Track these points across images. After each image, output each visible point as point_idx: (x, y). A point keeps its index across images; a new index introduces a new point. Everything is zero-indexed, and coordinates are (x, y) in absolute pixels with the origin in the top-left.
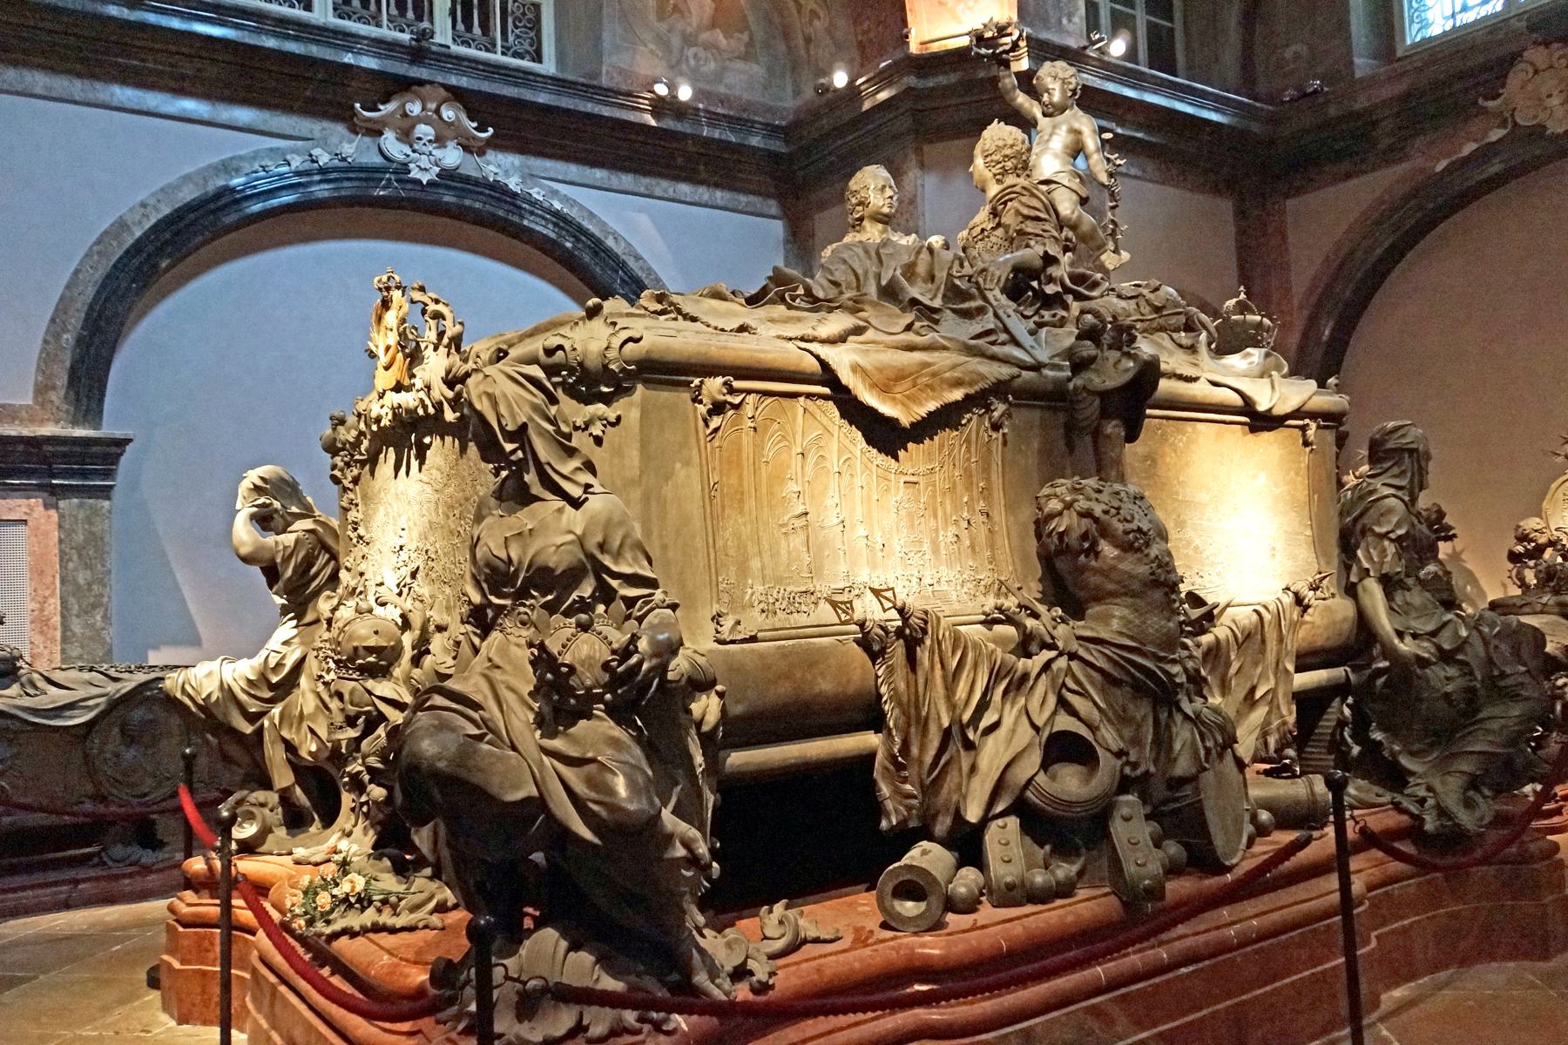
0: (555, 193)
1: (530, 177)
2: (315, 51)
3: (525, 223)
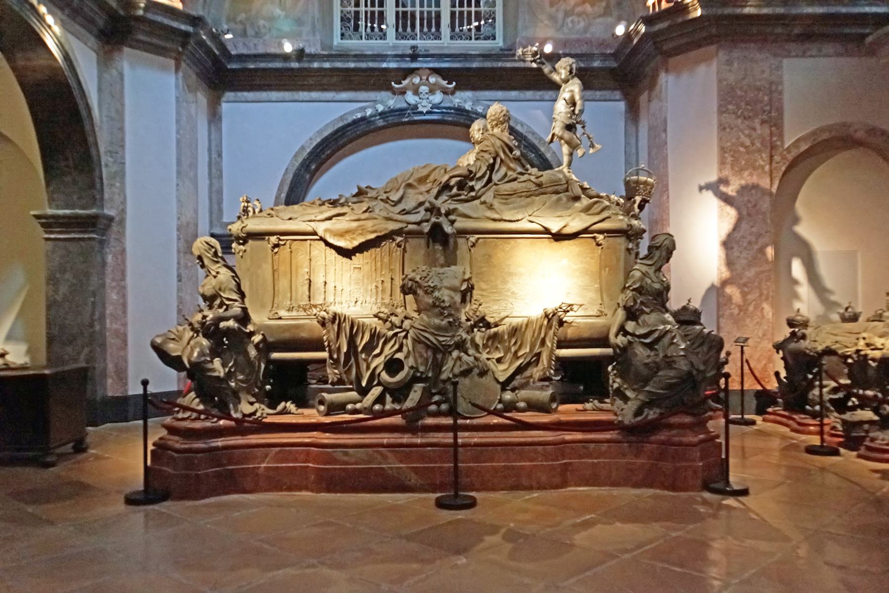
2: (371, 65)
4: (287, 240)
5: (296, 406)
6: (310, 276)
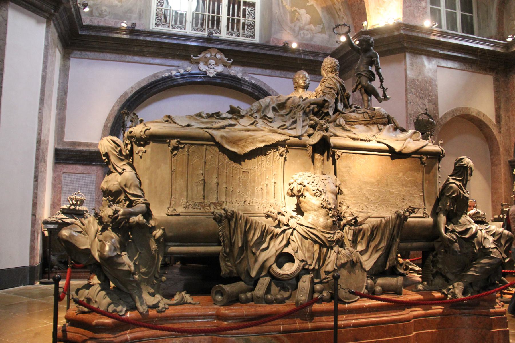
0: (253, 78)
1: (245, 73)
3: (243, 87)
4: (186, 144)
5: (191, 296)
6: (204, 177)
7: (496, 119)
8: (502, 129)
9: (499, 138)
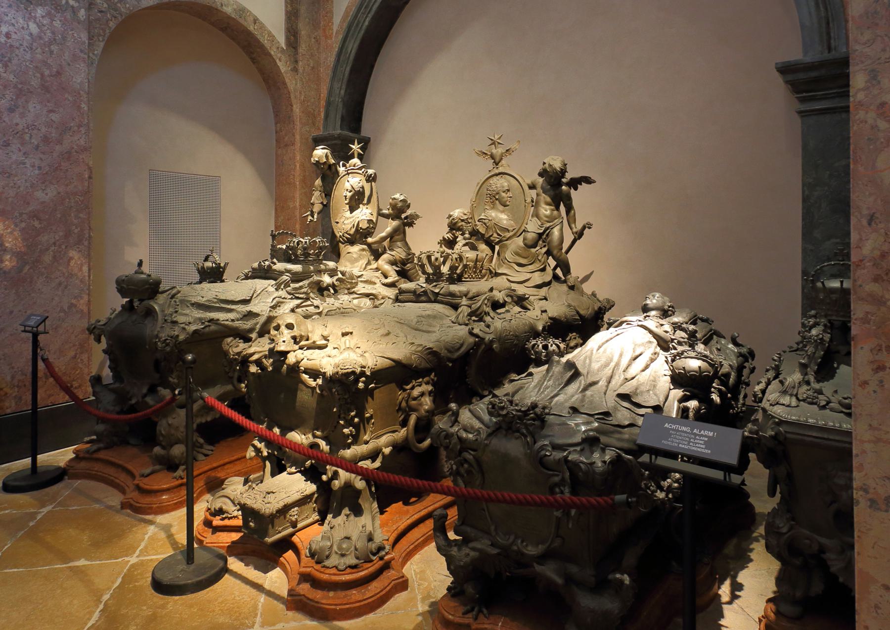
7: (287, 39)
8: (300, 63)
9: (292, 83)
